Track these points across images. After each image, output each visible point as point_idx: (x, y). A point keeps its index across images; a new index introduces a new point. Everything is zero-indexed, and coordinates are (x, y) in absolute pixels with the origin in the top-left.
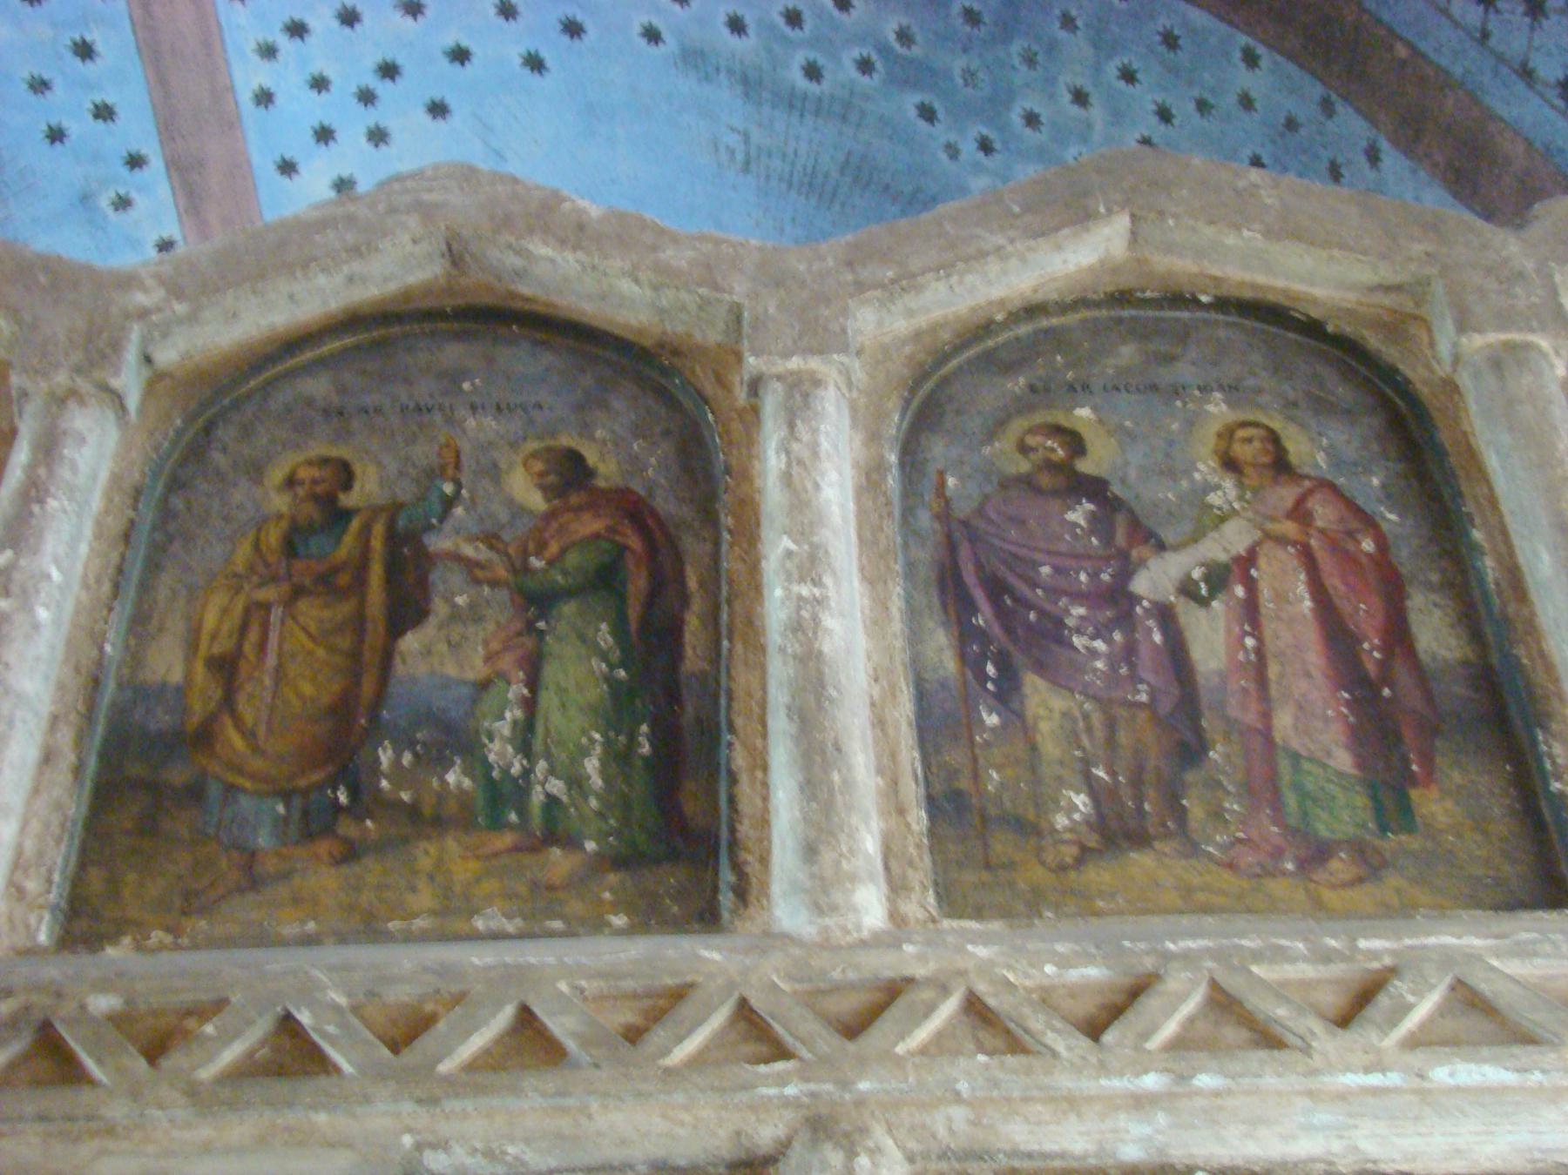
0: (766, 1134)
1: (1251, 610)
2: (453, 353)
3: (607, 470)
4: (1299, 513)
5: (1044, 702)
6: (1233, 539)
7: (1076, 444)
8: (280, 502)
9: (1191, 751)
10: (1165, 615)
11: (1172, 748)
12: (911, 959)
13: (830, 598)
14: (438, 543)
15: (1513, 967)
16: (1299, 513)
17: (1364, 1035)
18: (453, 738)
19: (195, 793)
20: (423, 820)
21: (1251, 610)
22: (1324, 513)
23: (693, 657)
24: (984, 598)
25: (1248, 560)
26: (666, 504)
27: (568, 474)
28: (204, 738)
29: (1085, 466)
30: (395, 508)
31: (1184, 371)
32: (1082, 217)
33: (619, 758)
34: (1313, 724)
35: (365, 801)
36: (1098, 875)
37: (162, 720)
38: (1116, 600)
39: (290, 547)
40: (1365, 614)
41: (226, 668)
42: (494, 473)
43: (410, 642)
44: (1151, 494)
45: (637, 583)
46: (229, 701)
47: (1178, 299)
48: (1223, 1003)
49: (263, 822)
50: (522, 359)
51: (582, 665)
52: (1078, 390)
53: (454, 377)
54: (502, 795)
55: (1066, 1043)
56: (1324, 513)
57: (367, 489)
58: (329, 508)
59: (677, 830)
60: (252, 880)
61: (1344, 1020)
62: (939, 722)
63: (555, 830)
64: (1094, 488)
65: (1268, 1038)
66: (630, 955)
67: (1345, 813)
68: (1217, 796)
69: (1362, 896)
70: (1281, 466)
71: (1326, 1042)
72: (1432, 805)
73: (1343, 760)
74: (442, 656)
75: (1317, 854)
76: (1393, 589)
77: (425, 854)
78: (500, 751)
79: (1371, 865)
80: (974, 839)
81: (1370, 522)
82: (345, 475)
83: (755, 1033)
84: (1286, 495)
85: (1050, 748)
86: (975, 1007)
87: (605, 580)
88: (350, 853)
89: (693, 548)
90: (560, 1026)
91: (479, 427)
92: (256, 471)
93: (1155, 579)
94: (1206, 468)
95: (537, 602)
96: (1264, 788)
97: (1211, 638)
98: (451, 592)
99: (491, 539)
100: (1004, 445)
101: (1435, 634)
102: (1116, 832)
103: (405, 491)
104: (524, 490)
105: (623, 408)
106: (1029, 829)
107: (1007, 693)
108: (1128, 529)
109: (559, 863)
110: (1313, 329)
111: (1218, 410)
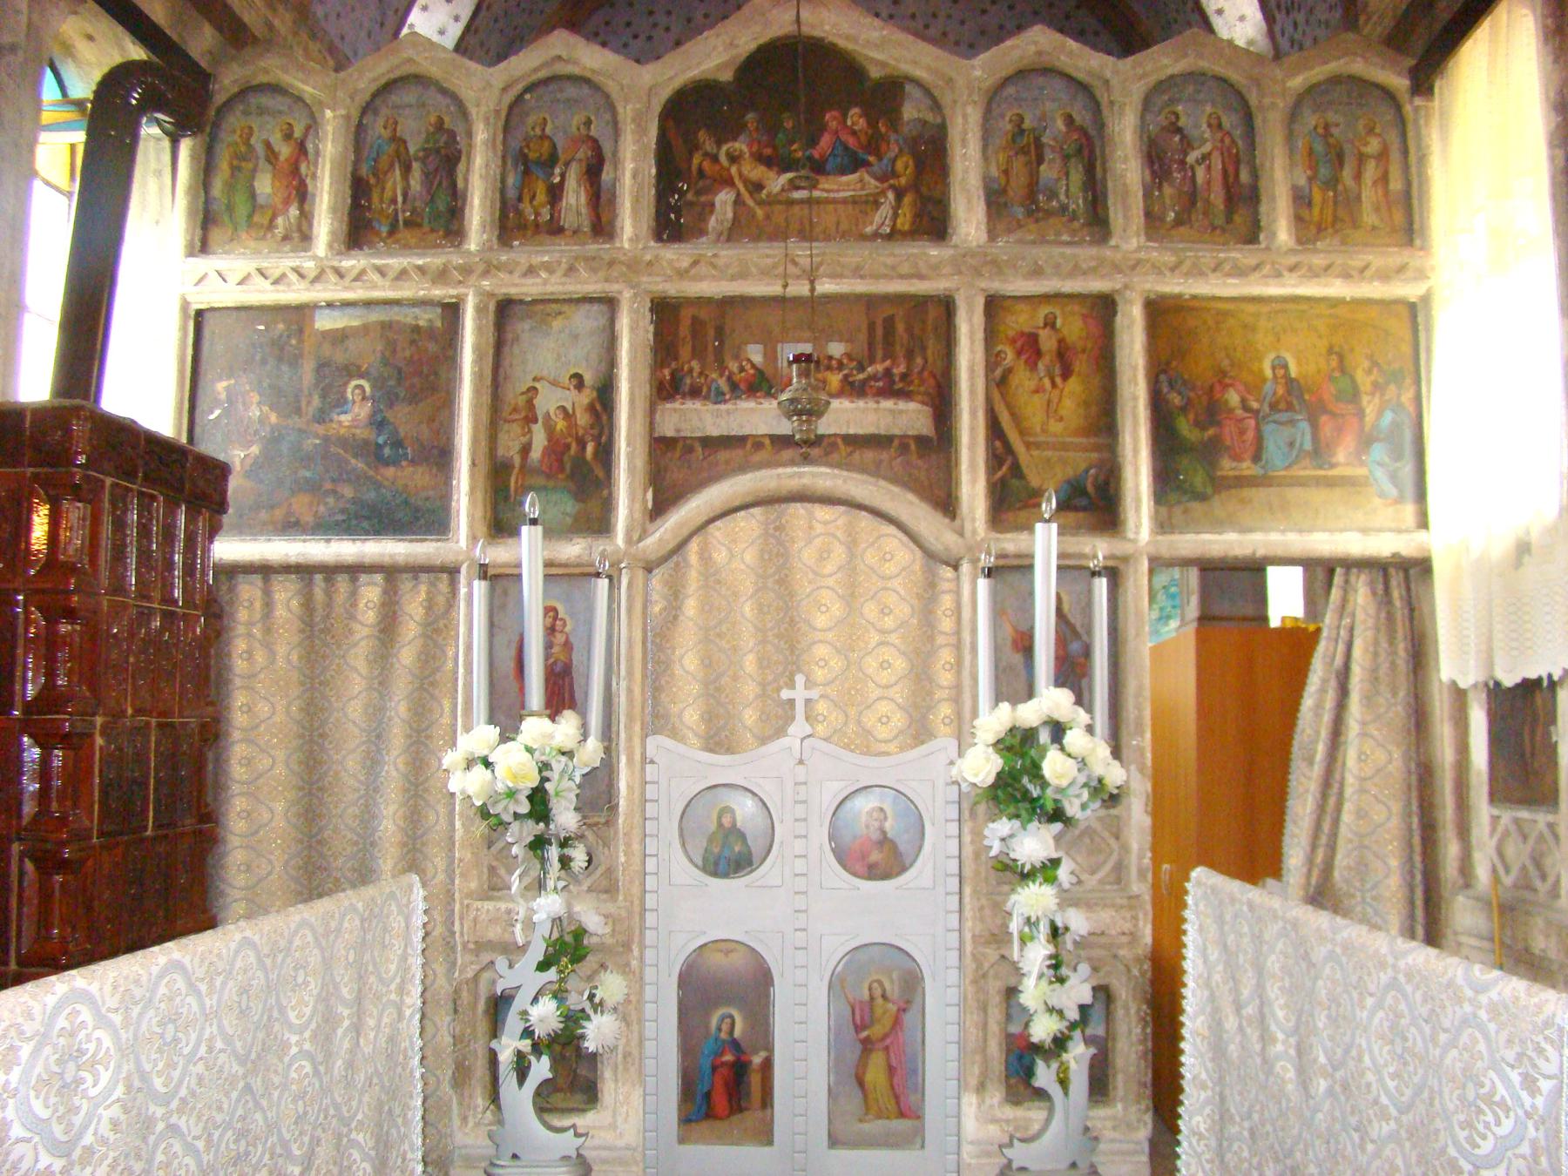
0: (1118, 286)
1: (1209, 168)
2: (1041, 80)
3: (1078, 119)
4: (1222, 141)
5: (1168, 190)
6: (1207, 148)
7: (1177, 117)
8: (1009, 127)
9: (1193, 203)
10: (1192, 168)
11: (1191, 198)
12: (1142, 255)
13: (1127, 169)
14: (1044, 140)
15: (1245, 261)
16: (1222, 141)
17: (1218, 274)
18: (1053, 195)
19: (1006, 204)
20: (1049, 214)
21: (1209, 168)
22: (1227, 141)
23: (1099, 174)
24: (1157, 160)
25: (1209, 154)
26: (1093, 133)
27: (1069, 120)
28: (1004, 191)
29: (1181, 123)
30: (1034, 130)
31: (1201, 96)
32: (1185, 55)
33: (1085, 199)
34: (1217, 198)
35: (1038, 209)
36: (1173, 232)
37: (996, 186)
38: (1182, 163)
39: (1014, 141)
40: (1231, 170)
41: (1006, 172)
42: (1053, 120)
43: (1042, 168)
44: (1194, 134)
45: (1086, 152)
46: (1008, 181)
47: (1204, 74)
48: (1194, 265)
49: (1019, 212)
50: (1058, 84)
51: (1077, 176)
52: (1179, 101)
53: (1042, 88)
54: (1064, 208)
55: (1168, 273)
56: (1227, 141)
57: (1027, 125)
58: (1020, 131)
59: (1097, 222)
60: (1020, 226)
61: (1214, 270)
62: (1147, 195)
63: (1073, 218)
64: (1179, 130)
65: (1202, 274)
66: (1093, 251)
67: (1220, 221)
68: (1197, 217)
69: (1221, 240)
70: (1220, 126)
71: (1211, 275)
72: (1238, 219)
73: (1222, 207)
74: (1048, 172)
75: (1214, 228)
76: (1237, 163)
77: (1051, 221)
78: (1062, 197)
79: (1224, 231)
80: (1153, 221)
81: (1233, 141)
82: (1021, 119)
83: (1117, 268)
84: (1219, 135)
85: (1168, 201)
86: (1154, 266)
87: (1079, 151)
88: (1037, 221)
89: (1097, 143)
90: (1084, 266)
91: (1049, 106)
92: (1003, 116)
93: (1191, 158)
94: (1204, 126)
95: (1066, 158)
96: (1206, 214)
97: (1200, 174)
98: (1049, 155)
99: (1055, 139)
100: (1162, 116)
101: (1244, 176)
102: (1178, 222)
103: (1035, 125)
104: (1060, 124)
105: (1081, 99)
106: (1162, 219)
107: (1160, 188)
108: (1187, 144)
109: (1076, 225)
110: (1232, 86)
111: (1209, 109)
